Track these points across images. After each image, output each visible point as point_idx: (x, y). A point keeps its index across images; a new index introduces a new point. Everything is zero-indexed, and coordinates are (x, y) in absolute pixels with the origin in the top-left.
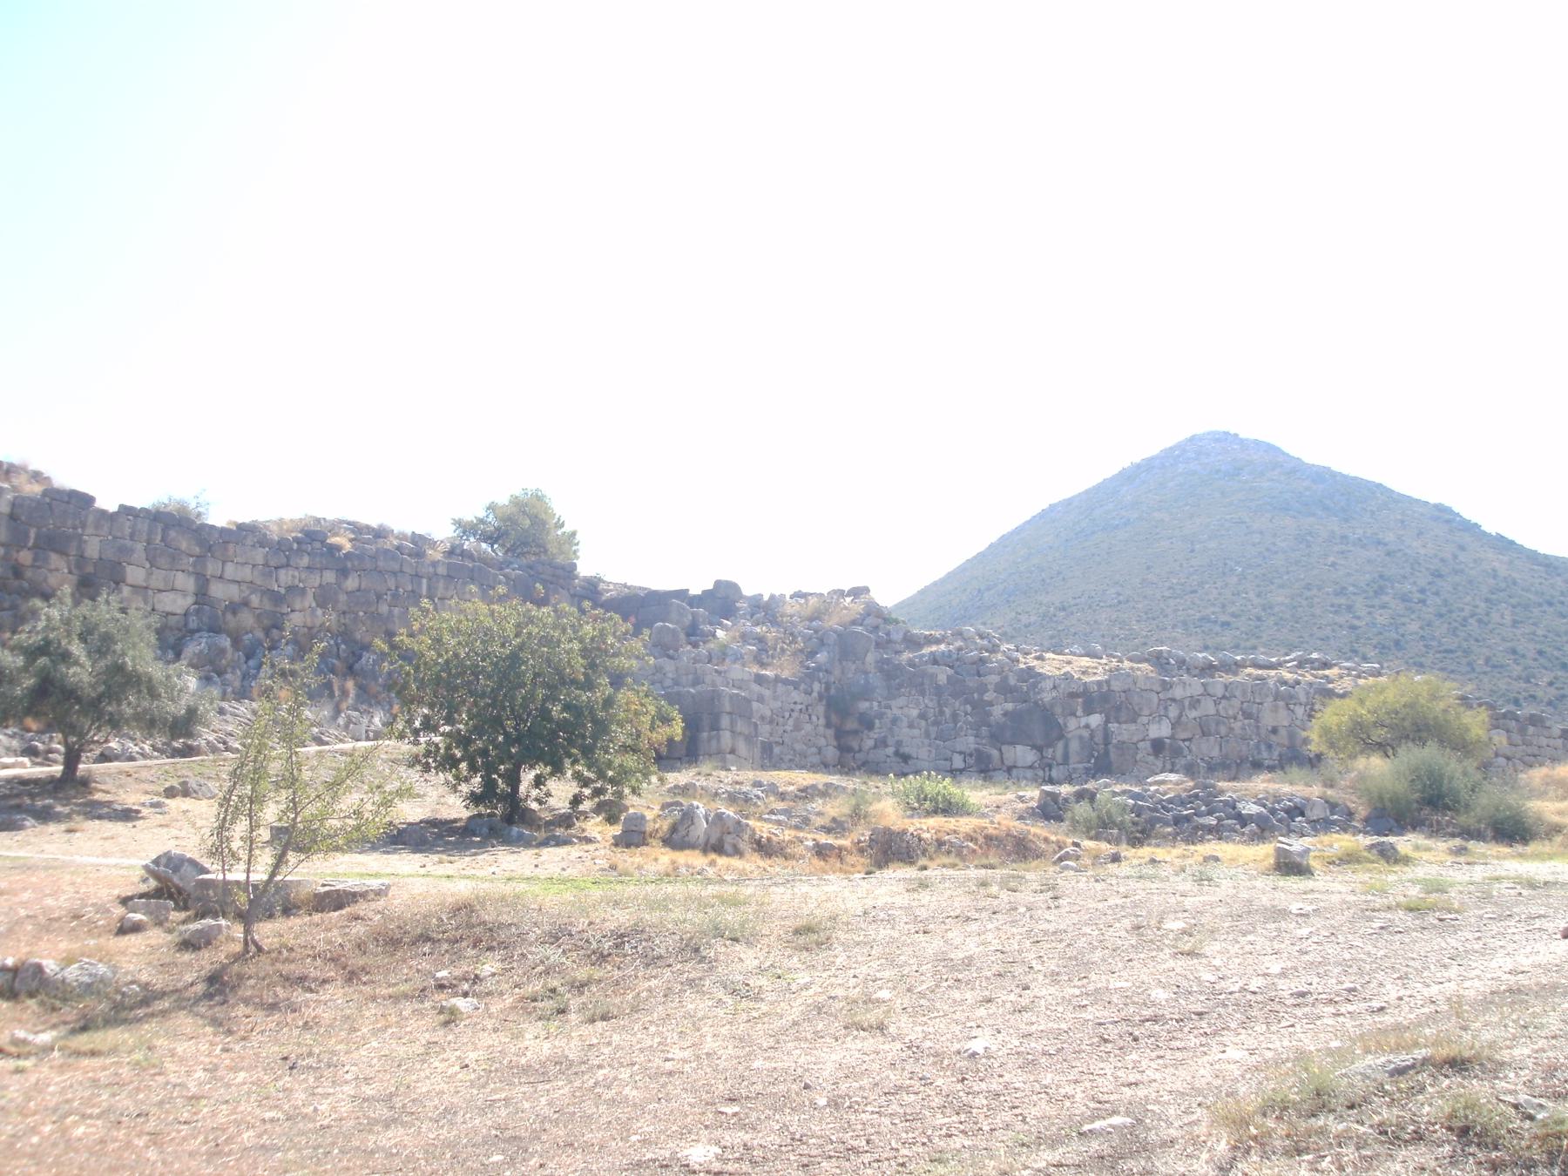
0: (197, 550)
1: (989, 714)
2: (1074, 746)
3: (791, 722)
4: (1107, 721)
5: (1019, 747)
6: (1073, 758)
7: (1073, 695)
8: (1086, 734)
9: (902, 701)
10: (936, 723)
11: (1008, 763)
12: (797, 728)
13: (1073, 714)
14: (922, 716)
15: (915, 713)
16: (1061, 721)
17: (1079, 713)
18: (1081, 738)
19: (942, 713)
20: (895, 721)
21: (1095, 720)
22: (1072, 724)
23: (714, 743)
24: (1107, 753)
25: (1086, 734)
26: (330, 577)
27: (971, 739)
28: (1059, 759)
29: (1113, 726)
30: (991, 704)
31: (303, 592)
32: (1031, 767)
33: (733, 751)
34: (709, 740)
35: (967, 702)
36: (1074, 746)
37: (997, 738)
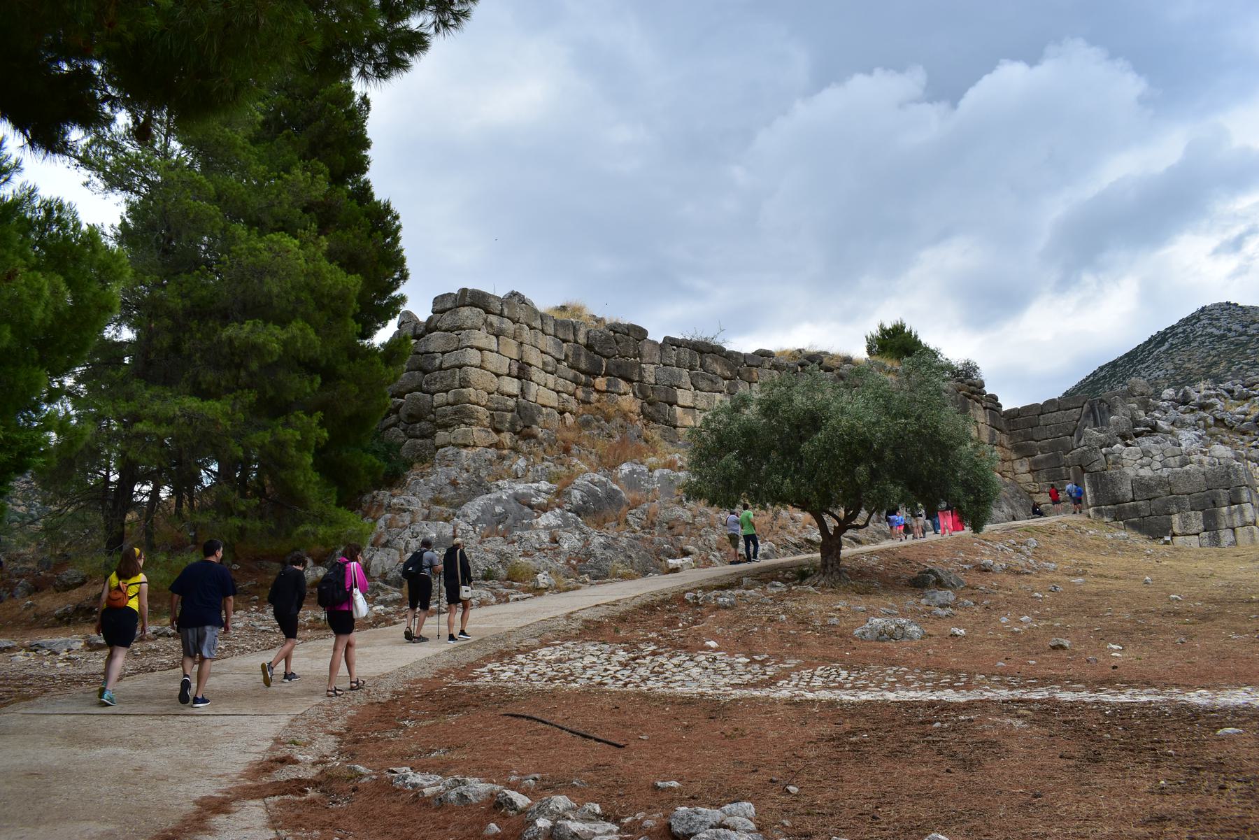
0: (728, 374)
23: (1237, 517)
34: (1231, 514)
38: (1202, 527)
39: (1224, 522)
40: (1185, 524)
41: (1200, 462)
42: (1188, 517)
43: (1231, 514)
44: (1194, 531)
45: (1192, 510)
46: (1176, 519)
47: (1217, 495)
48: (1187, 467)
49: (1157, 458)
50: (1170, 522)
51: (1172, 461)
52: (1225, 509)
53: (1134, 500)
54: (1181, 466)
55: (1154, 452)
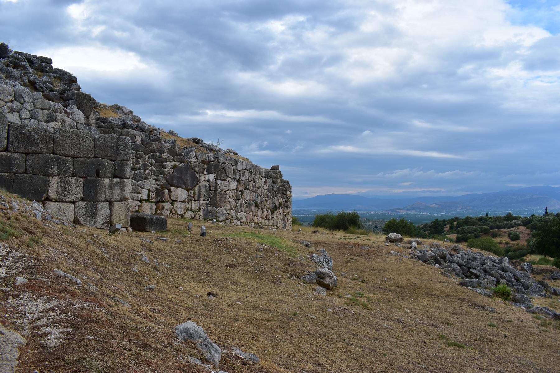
1: (164, 167)
2: (203, 191)
4: (216, 179)
5: (180, 189)
6: (202, 197)
7: (203, 162)
11: (173, 198)
13: (203, 173)
16: (197, 175)
17: (205, 172)
18: (206, 186)
19: (137, 162)
21: (212, 177)
22: (202, 178)
23: (117, 191)
24: (215, 195)
27: (154, 181)
28: (196, 197)
29: (219, 182)
30: (166, 160)
32: (183, 202)
34: (112, 187)
35: (153, 157)
36: (203, 191)
38: (80, 195)
39: (105, 194)
40: (64, 188)
41: (63, 122)
42: (68, 182)
43: (112, 187)
44: (72, 198)
45: (74, 175)
46: (54, 182)
47: (103, 164)
48: (52, 124)
49: (28, 106)
50: (47, 185)
51: (40, 114)
52: (107, 181)
53: (6, 150)
54: (47, 122)
55: (26, 99)
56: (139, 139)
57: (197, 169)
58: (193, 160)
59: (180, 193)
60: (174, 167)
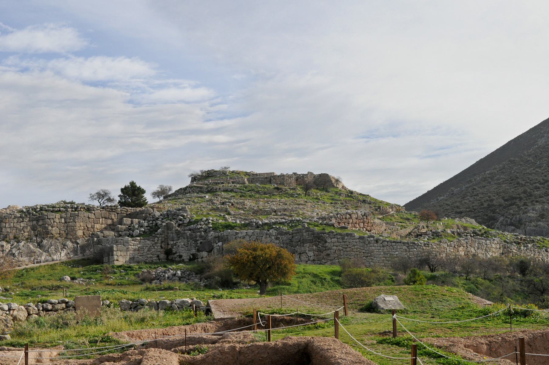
3: (146, 249)
7: (215, 237)
8: (218, 248)
9: (180, 241)
10: (187, 246)
12: (149, 250)
14: (184, 245)
15: (183, 244)
20: (179, 246)
21: (220, 244)
22: (215, 245)
25: (218, 248)
26: (35, 222)
31: (27, 228)
33: (117, 260)
36: (216, 251)
37: (198, 250)
56: (188, 234)
57: (212, 241)
58: (210, 238)
59: (205, 254)
60: (201, 243)
